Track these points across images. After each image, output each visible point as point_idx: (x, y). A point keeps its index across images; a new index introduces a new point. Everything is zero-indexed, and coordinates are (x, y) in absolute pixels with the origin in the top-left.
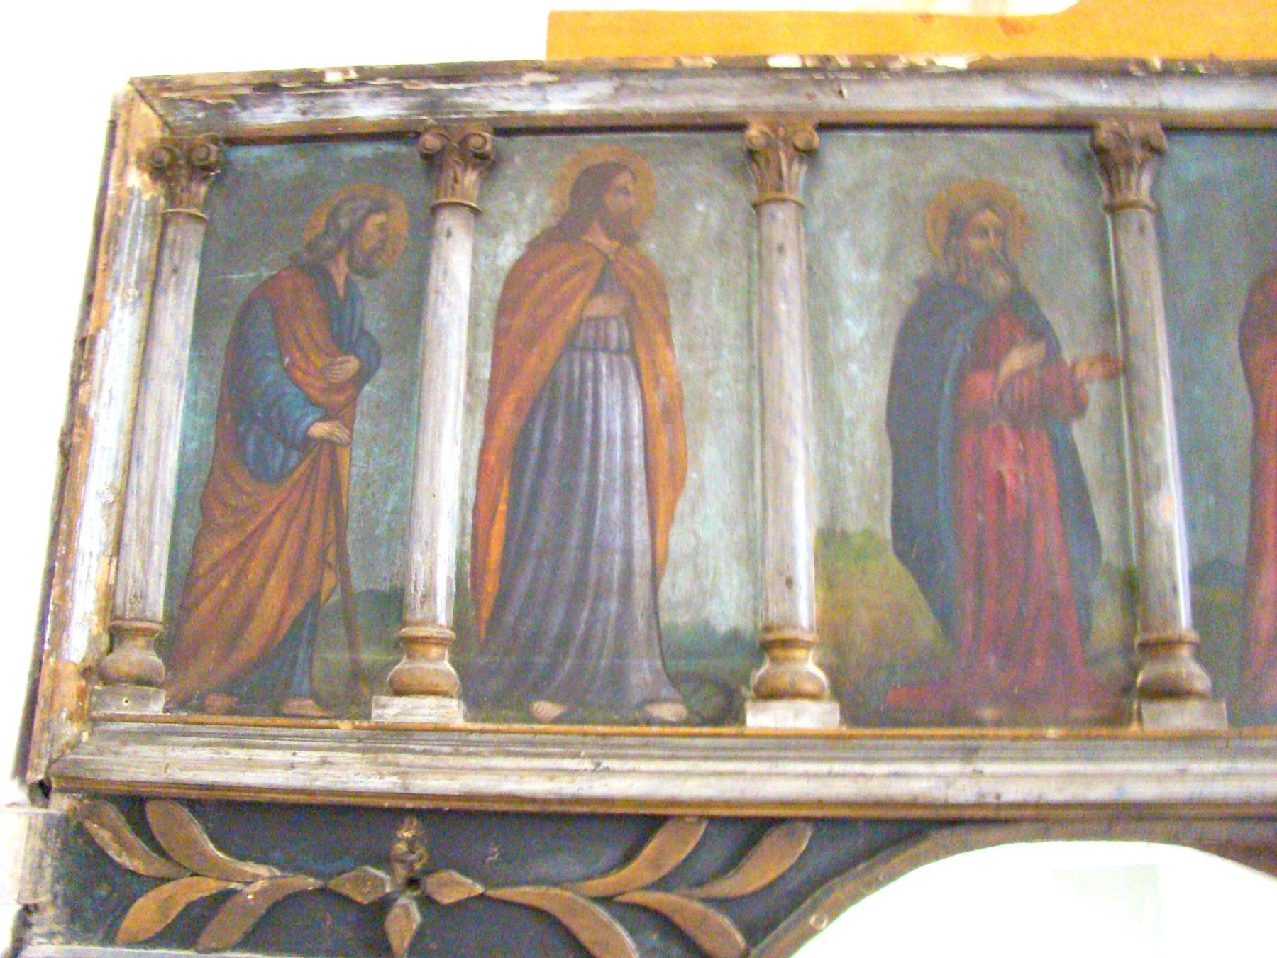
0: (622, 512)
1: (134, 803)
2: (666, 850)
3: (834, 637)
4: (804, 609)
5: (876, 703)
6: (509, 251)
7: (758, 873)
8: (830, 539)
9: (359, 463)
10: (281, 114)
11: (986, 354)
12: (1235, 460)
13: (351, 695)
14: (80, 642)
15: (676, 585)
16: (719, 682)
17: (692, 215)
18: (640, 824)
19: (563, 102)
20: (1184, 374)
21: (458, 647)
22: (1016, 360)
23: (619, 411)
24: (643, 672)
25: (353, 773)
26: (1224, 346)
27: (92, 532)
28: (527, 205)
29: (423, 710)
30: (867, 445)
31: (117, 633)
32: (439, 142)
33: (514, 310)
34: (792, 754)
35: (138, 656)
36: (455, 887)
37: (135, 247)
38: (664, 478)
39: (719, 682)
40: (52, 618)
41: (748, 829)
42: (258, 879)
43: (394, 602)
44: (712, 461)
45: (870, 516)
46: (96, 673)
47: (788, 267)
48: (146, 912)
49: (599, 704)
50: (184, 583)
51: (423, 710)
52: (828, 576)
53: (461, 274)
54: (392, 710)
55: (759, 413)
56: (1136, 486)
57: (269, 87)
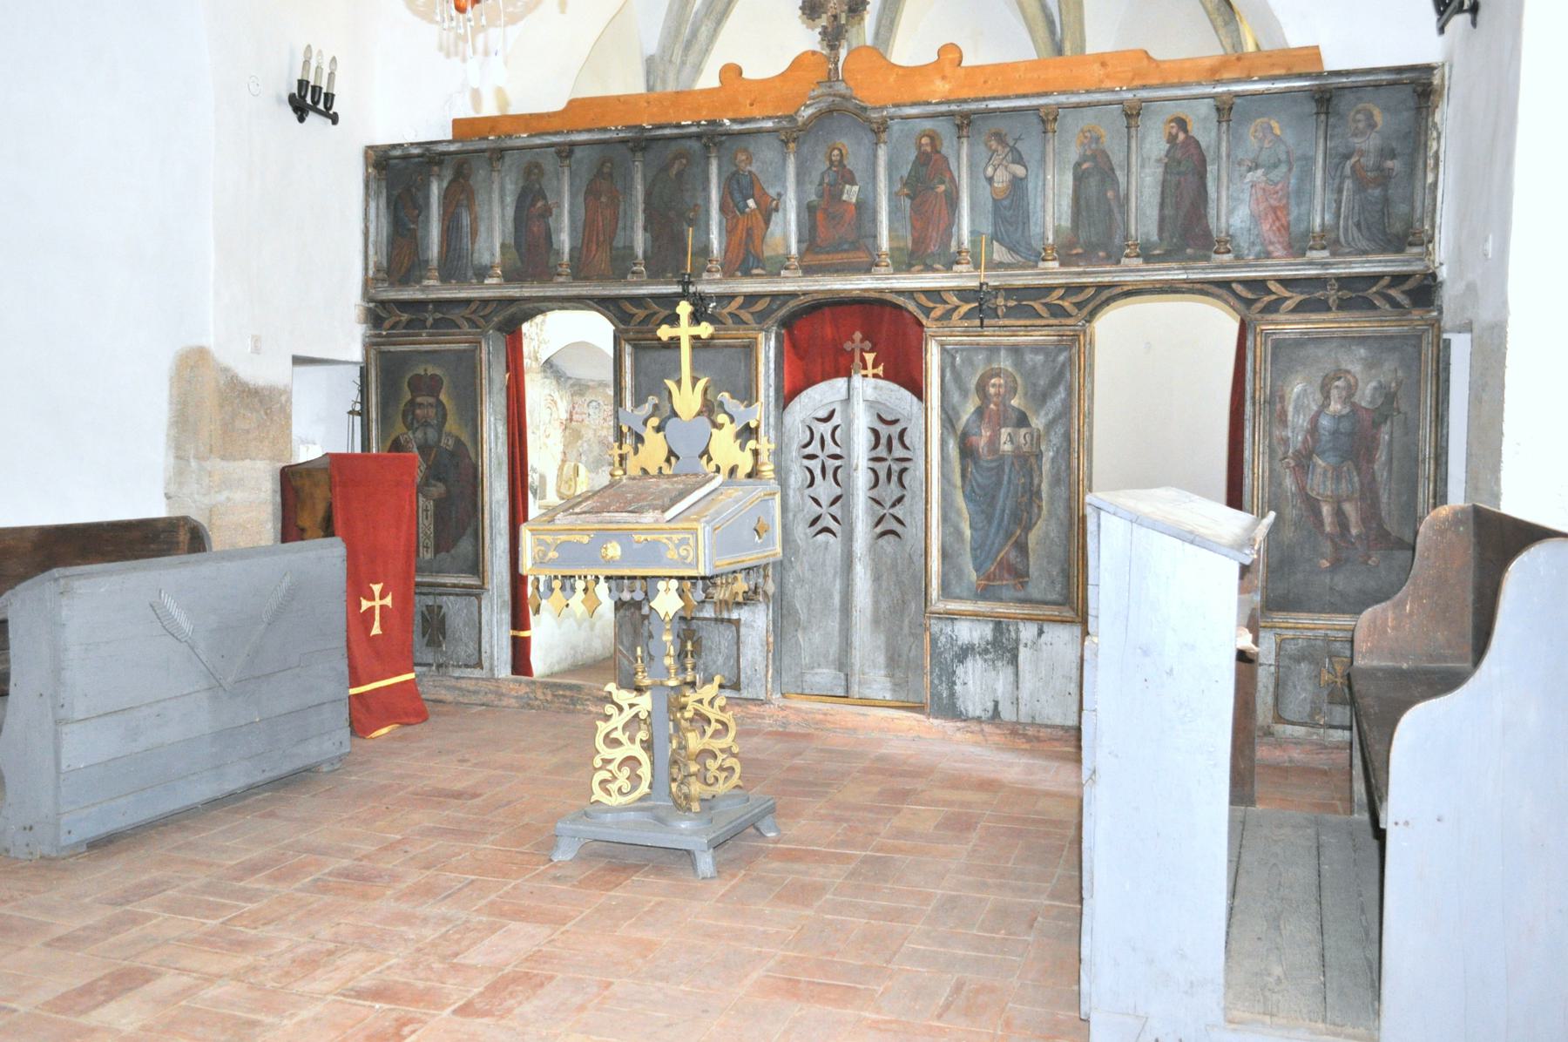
0: (466, 241)
1: (383, 303)
2: (473, 307)
3: (503, 265)
4: (498, 259)
5: (510, 277)
6: (445, 184)
7: (487, 311)
8: (503, 246)
9: (419, 234)
10: (398, 153)
11: (533, 205)
12: (580, 224)
13: (419, 281)
14: (371, 273)
15: (476, 255)
16: (482, 273)
17: (480, 175)
18: (467, 302)
19: (453, 148)
20: (572, 205)
21: (440, 268)
22: (539, 204)
23: (466, 220)
24: (470, 274)
25: (420, 296)
26: (581, 199)
27: (371, 251)
28: (448, 174)
29: (431, 282)
30: (510, 225)
31: (378, 270)
32: (427, 158)
33: (446, 197)
34: (493, 287)
35: (382, 275)
36: (439, 315)
37: (373, 185)
38: (474, 233)
39: (482, 273)
40: (366, 269)
41: (485, 302)
42: (405, 317)
43: (427, 262)
44: (482, 228)
45: (510, 241)
46: (376, 279)
47: (496, 186)
48: (387, 324)
49: (463, 280)
50: (390, 260)
51: (431, 282)
52: (503, 254)
53: (435, 190)
54: (426, 282)
55: (491, 218)
56: (559, 231)
57: (394, 147)
